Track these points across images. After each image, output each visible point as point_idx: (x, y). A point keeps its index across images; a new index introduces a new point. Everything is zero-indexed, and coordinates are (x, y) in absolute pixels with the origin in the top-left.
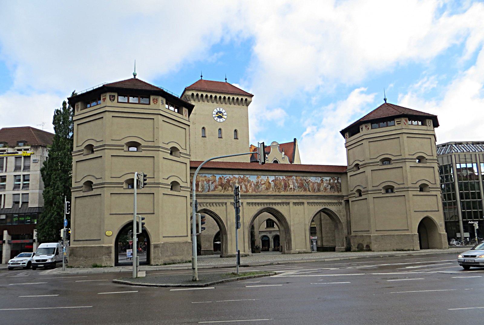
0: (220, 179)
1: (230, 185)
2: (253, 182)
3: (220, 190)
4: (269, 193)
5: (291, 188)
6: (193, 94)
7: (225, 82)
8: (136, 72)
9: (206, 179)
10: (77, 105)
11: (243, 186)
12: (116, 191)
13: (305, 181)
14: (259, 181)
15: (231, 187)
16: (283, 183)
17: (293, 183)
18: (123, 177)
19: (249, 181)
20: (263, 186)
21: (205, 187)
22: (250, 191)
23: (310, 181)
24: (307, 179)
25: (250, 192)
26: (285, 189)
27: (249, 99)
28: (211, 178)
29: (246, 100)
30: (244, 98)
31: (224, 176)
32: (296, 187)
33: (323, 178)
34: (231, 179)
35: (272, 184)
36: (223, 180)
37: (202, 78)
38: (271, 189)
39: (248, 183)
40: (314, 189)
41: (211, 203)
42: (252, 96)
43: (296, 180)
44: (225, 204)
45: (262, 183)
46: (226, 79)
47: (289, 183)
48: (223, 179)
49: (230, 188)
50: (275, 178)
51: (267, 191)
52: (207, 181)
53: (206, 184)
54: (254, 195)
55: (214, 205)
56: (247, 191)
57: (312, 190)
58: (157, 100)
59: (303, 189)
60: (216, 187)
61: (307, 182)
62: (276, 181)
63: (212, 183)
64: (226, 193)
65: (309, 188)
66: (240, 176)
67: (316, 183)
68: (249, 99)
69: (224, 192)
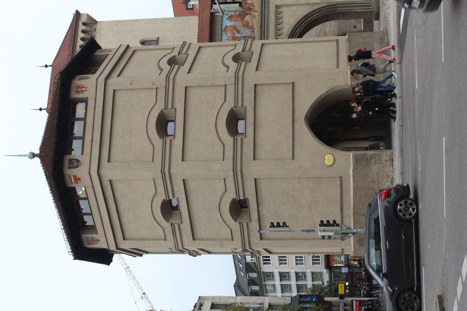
3: (252, 18)
7: (51, 68)
8: (27, 152)
10: (88, 244)
12: (248, 150)
18: (223, 139)
27: (83, 19)
28: (228, 35)
29: (84, 24)
30: (81, 27)
37: (44, 109)
41: (276, 33)
42: (78, 15)
44: (279, 8)
46: (46, 66)
55: (280, 27)
58: (79, 87)
60: (247, 25)
63: (238, 32)
68: (83, 19)
69: (256, 11)
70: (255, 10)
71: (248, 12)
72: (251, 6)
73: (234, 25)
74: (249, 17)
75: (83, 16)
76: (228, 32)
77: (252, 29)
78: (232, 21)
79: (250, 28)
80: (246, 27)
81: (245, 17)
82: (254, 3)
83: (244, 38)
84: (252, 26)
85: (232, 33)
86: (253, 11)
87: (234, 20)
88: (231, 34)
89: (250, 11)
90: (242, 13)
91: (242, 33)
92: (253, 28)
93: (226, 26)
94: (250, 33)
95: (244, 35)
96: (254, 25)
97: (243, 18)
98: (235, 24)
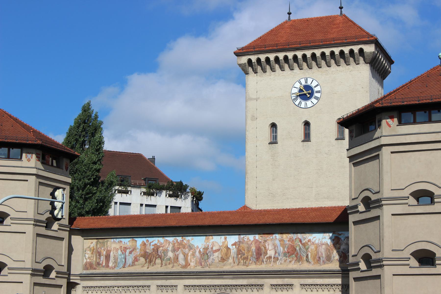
0: (144, 245)
1: (159, 256)
2: (198, 247)
3: (142, 264)
4: (227, 268)
5: (270, 257)
6: (250, 61)
7: (339, 14)
9: (121, 247)
11: (181, 257)
13: (301, 241)
14: (208, 246)
15: (161, 258)
16: (253, 248)
17: (275, 246)
19: (190, 247)
20: (216, 254)
21: (119, 260)
22: (192, 264)
23: (309, 241)
24: (305, 239)
25: (193, 267)
26: (258, 259)
28: (128, 244)
30: (356, 49)
31: (150, 240)
32: (279, 255)
33: (340, 235)
34: (161, 244)
35: (234, 250)
36: (148, 247)
38: (231, 260)
39: (189, 251)
40: (319, 258)
43: (281, 240)
45: (214, 249)
47: (265, 248)
48: (148, 245)
49: (158, 261)
50: (239, 238)
51: (222, 264)
52: (122, 249)
53: (120, 255)
54: (197, 272)
56: (187, 264)
57: (314, 259)
59: (295, 258)
60: (136, 259)
61: (304, 245)
62: (241, 245)
63: (130, 253)
64: (152, 269)
65: (307, 256)
66: (175, 239)
67: (323, 244)
69: (148, 268)
70: (149, 267)
71: (148, 260)
72: (153, 263)
73: (137, 248)
74: (143, 262)
75: (370, 47)
76: (131, 243)
77: (132, 265)
78: (140, 246)
79: (134, 263)
80: (134, 259)
81: (143, 257)
82: (156, 266)
83: (125, 258)
84: (135, 265)
85: (130, 246)
86: (149, 265)
87: (142, 248)
88: (129, 246)
89: (149, 262)
90: (147, 255)
91: (129, 255)
92: (133, 266)
93: (137, 241)
94: (128, 263)
95: (127, 257)
96: (136, 266)
97: (143, 256)
98: (138, 249)
